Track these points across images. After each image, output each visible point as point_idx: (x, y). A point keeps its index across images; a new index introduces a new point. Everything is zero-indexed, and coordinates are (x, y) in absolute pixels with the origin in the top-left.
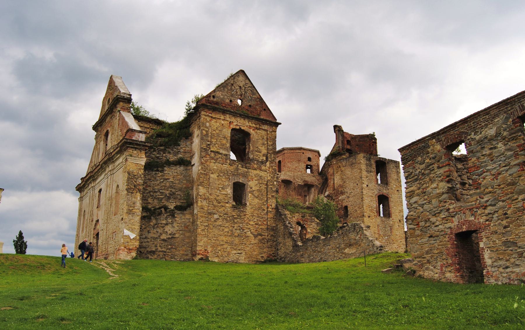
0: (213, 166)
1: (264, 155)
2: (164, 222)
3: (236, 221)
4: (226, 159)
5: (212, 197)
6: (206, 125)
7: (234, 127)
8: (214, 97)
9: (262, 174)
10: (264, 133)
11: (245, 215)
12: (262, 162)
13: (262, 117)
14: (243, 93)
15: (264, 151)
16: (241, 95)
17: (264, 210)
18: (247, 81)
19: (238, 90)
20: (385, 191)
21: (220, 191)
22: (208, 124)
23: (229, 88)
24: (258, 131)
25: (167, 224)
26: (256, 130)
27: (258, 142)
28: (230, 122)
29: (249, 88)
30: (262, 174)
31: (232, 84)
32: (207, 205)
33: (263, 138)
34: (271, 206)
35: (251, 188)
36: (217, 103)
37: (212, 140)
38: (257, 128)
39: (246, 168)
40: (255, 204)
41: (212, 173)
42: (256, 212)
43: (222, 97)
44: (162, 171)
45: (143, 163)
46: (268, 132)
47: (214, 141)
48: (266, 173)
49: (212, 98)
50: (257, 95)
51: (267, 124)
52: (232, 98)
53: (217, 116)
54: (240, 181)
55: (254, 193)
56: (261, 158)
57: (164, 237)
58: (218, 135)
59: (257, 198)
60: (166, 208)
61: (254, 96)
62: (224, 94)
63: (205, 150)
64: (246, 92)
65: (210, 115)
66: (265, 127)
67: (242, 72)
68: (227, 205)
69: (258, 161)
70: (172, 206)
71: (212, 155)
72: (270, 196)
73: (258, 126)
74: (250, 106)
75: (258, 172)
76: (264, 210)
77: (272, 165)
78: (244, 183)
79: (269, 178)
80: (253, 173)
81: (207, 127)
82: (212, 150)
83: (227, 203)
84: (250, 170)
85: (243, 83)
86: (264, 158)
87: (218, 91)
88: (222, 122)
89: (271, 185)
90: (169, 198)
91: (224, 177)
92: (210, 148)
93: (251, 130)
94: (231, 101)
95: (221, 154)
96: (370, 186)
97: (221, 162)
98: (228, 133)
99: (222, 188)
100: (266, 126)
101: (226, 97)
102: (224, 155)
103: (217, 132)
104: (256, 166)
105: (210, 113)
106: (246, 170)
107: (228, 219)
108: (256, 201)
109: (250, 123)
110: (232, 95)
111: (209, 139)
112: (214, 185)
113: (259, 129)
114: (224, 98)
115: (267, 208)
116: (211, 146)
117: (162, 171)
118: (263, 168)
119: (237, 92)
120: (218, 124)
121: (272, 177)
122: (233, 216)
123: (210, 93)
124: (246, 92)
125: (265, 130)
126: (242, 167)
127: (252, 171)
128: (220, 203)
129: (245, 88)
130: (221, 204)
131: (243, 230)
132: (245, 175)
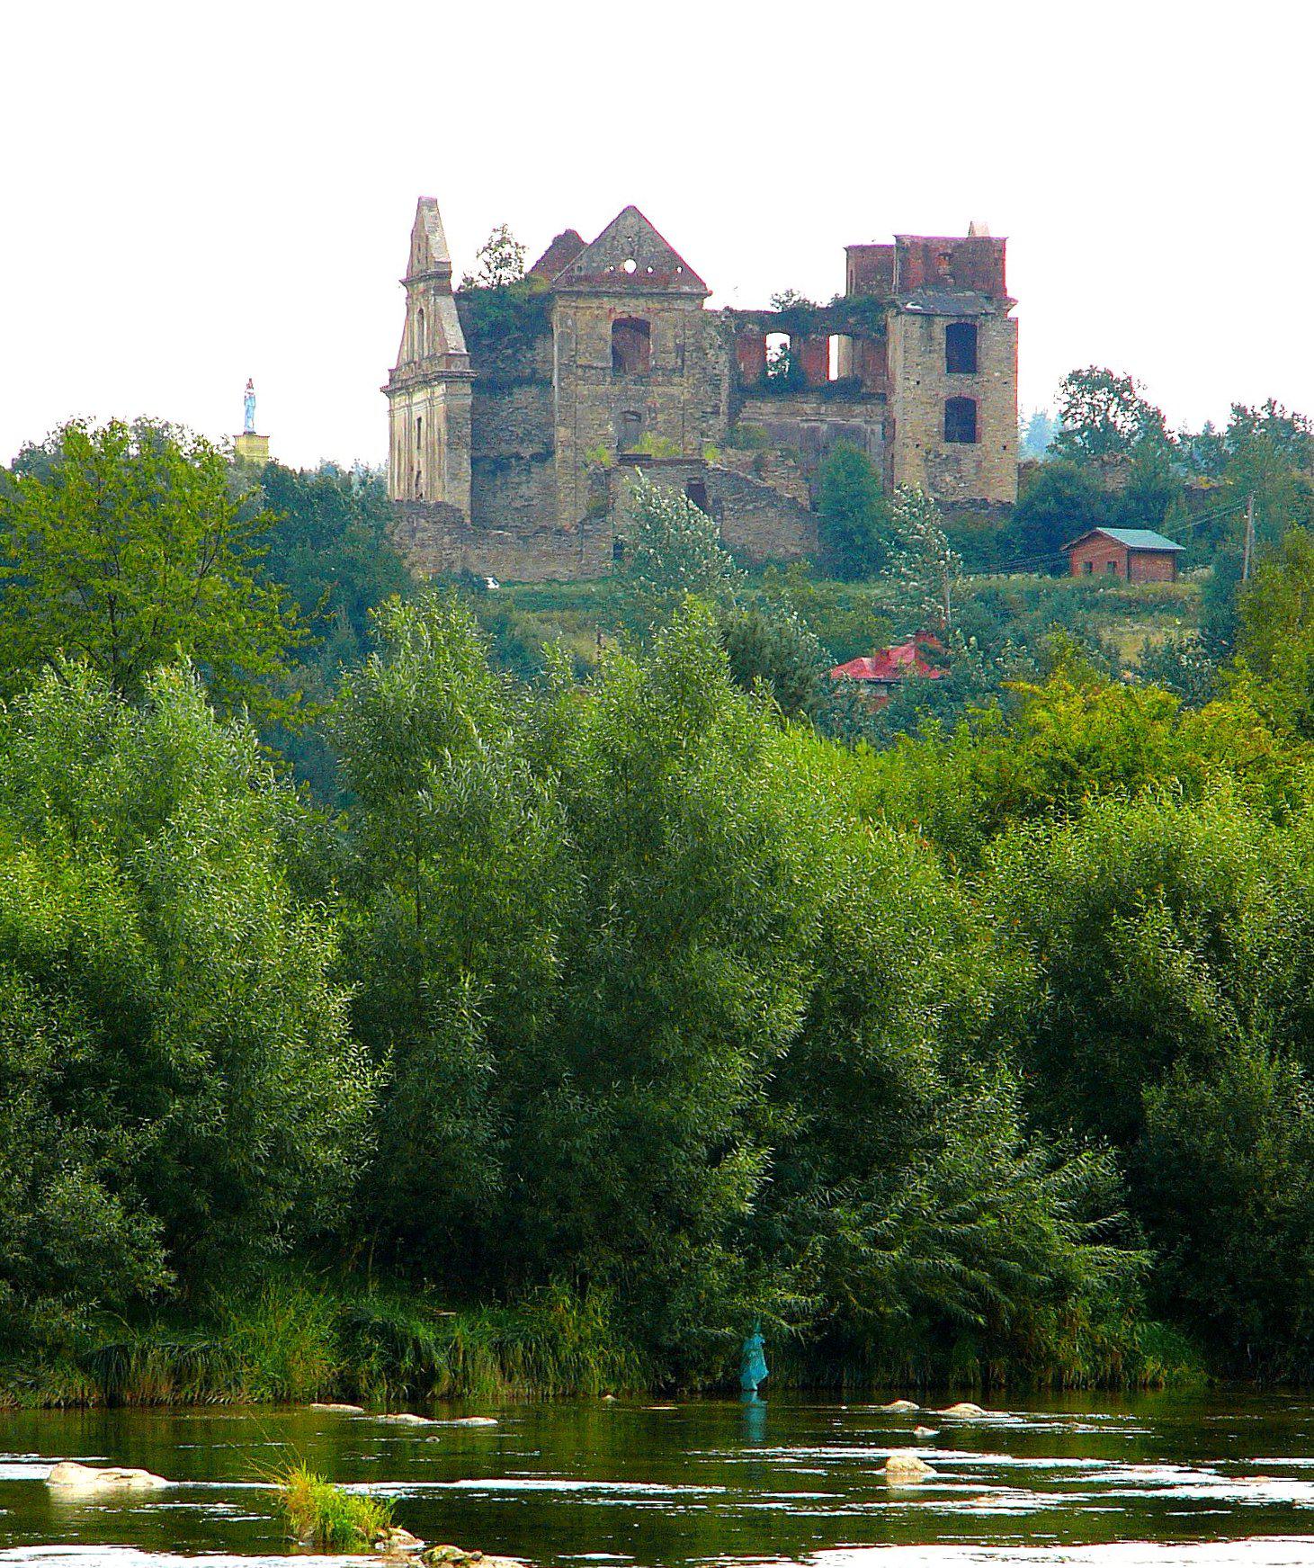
0: (583, 389)
2: (517, 480)
25: (519, 484)
30: (675, 390)
44: (510, 394)
45: (469, 401)
57: (518, 504)
60: (518, 457)
63: (566, 368)
64: (641, 246)
67: (631, 211)
70: (527, 452)
79: (687, 396)
90: (522, 441)
98: (606, 329)
117: (510, 394)
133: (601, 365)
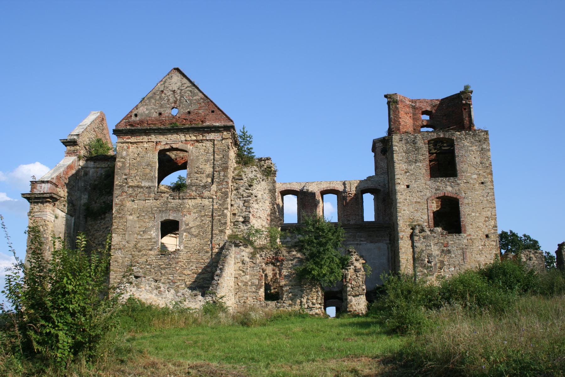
1: (208, 176)
3: (163, 272)
4: (149, 193)
5: (130, 245)
6: (122, 155)
7: (163, 148)
8: (136, 115)
9: (206, 202)
10: (209, 144)
11: (177, 263)
12: (205, 187)
13: (207, 124)
14: (178, 98)
15: (209, 169)
16: (175, 102)
17: (207, 252)
18: (185, 80)
19: (170, 97)
20: (449, 189)
21: (141, 235)
22: (124, 153)
23: (158, 97)
24: (201, 144)
26: (197, 144)
27: (198, 159)
28: (157, 143)
29: (188, 89)
31: (162, 91)
32: (122, 256)
33: (208, 153)
34: (219, 245)
35: (188, 225)
36: (141, 122)
37: (131, 172)
38: (197, 141)
39: (179, 199)
40: (193, 245)
41: (131, 214)
42: (195, 256)
43: (147, 112)
46: (216, 142)
47: (133, 172)
48: (211, 200)
49: (133, 118)
50: (200, 94)
51: (214, 132)
52: (162, 110)
53: (140, 139)
54: (171, 218)
55: (193, 230)
56: (204, 181)
58: (139, 163)
59: (196, 236)
61: (195, 98)
62: (149, 107)
65: (128, 140)
66: (212, 136)
67: (178, 70)
68: (152, 252)
69: (197, 186)
71: (130, 191)
72: (217, 232)
73: (200, 137)
74: (189, 112)
75: (199, 200)
76: (207, 252)
77: (221, 186)
78: (177, 219)
79: (216, 207)
80: (191, 203)
81: (124, 158)
82: (130, 184)
83: (151, 250)
84: (186, 201)
85: (179, 84)
86: (209, 180)
87: (143, 106)
88: (146, 145)
89: (219, 216)
91: (146, 217)
92: (127, 183)
93: (189, 146)
94: (160, 114)
95: (142, 187)
96: (413, 185)
97: (143, 198)
99: (144, 232)
100: (213, 134)
101: (153, 111)
102: (147, 188)
103: (138, 159)
104: (194, 194)
105: (128, 139)
106: (180, 201)
107: (153, 270)
108: (195, 240)
109: (187, 136)
110: (161, 106)
111: (127, 171)
112: (133, 230)
113: (202, 141)
114: (150, 113)
115: (212, 249)
116: (129, 180)
118: (206, 193)
119: (169, 100)
120: (140, 149)
121: (220, 205)
122: (160, 265)
123: (131, 112)
124: (182, 96)
125: (211, 140)
126: (173, 199)
127: (190, 201)
128: (140, 251)
129: (181, 90)
130: (142, 253)
131: (175, 283)
132: (177, 209)
133: (147, 184)
